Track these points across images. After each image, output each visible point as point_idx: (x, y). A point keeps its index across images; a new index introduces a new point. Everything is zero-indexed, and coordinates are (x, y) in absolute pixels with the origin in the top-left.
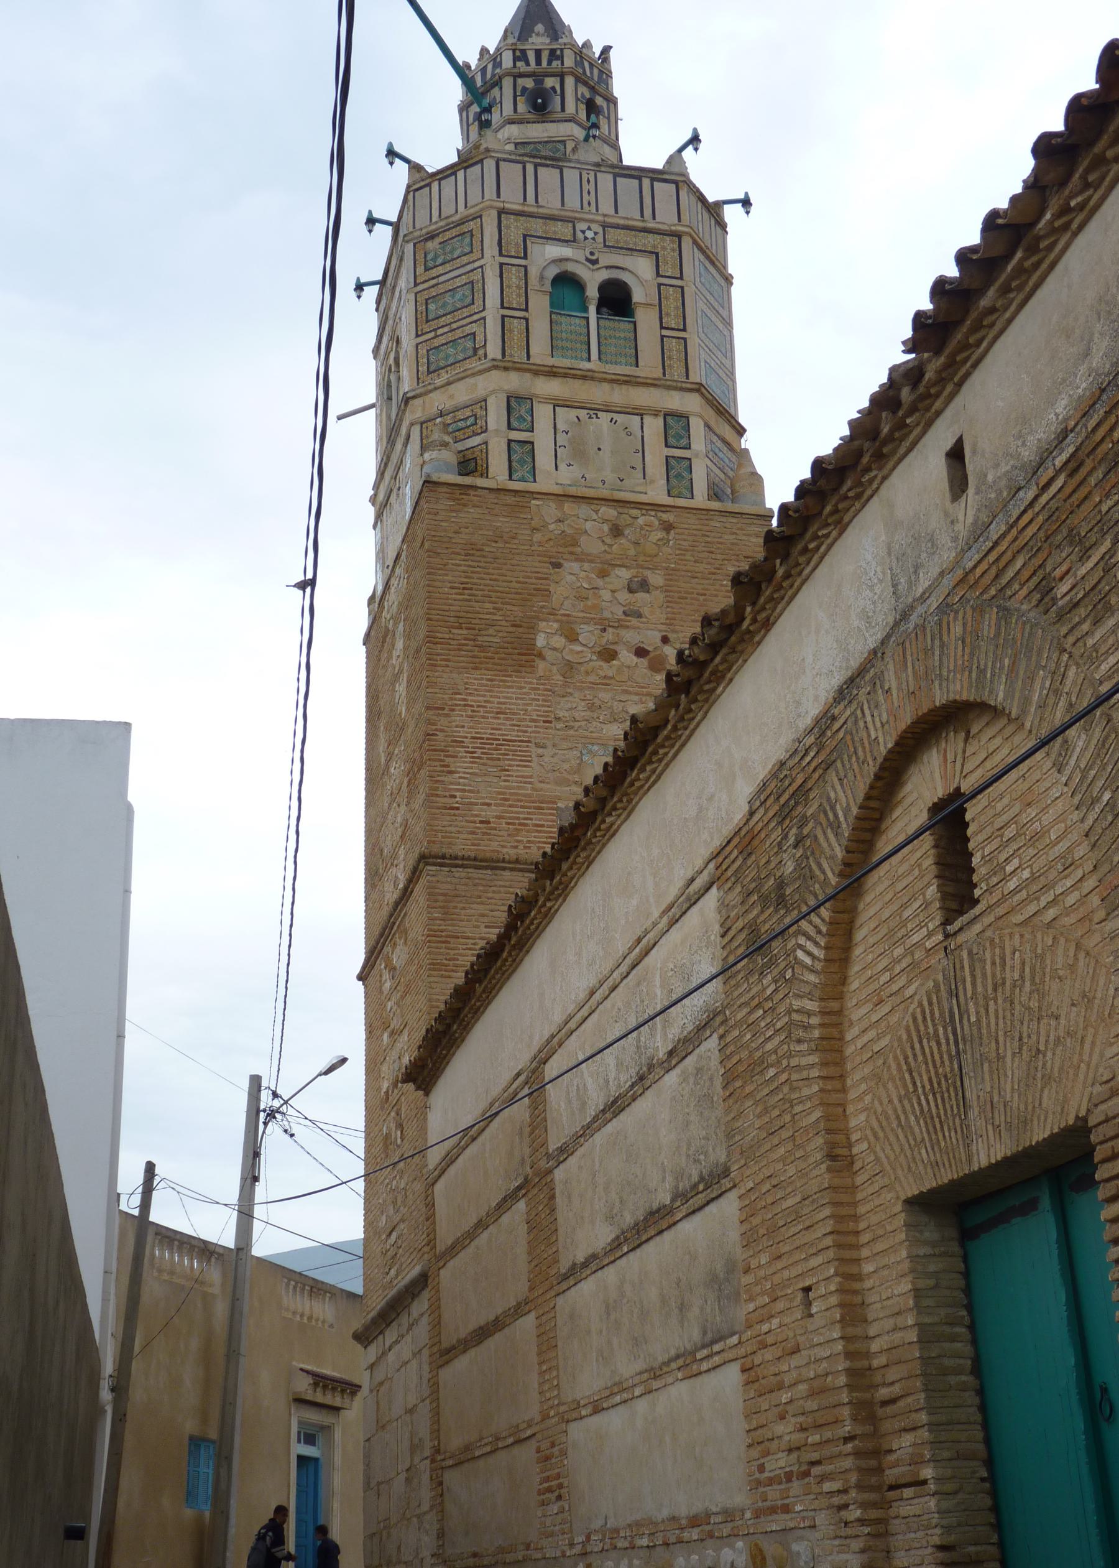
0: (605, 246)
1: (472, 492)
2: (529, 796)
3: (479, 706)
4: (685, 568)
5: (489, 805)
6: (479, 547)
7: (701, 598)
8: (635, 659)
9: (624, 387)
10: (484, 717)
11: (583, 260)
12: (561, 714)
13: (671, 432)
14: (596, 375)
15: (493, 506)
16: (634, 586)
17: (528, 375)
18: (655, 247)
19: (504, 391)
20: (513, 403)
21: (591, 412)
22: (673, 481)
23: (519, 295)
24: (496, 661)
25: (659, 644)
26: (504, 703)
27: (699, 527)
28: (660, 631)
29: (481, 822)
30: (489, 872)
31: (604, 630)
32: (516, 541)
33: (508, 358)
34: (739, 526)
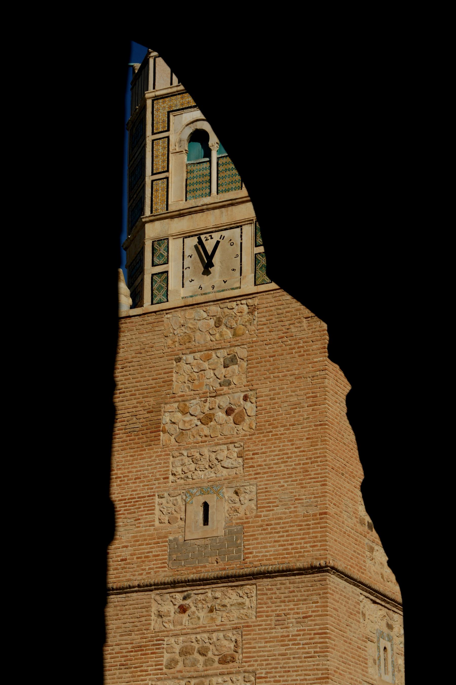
2: (152, 535)
3: (124, 477)
4: (262, 339)
5: (126, 547)
9: (230, 208)
10: (127, 484)
15: (140, 327)
16: (228, 362)
17: (167, 220)
20: (156, 246)
21: (207, 235)
23: (163, 161)
24: (137, 441)
25: (242, 402)
26: (140, 471)
29: (122, 560)
30: (124, 595)
32: (153, 349)
33: (155, 213)
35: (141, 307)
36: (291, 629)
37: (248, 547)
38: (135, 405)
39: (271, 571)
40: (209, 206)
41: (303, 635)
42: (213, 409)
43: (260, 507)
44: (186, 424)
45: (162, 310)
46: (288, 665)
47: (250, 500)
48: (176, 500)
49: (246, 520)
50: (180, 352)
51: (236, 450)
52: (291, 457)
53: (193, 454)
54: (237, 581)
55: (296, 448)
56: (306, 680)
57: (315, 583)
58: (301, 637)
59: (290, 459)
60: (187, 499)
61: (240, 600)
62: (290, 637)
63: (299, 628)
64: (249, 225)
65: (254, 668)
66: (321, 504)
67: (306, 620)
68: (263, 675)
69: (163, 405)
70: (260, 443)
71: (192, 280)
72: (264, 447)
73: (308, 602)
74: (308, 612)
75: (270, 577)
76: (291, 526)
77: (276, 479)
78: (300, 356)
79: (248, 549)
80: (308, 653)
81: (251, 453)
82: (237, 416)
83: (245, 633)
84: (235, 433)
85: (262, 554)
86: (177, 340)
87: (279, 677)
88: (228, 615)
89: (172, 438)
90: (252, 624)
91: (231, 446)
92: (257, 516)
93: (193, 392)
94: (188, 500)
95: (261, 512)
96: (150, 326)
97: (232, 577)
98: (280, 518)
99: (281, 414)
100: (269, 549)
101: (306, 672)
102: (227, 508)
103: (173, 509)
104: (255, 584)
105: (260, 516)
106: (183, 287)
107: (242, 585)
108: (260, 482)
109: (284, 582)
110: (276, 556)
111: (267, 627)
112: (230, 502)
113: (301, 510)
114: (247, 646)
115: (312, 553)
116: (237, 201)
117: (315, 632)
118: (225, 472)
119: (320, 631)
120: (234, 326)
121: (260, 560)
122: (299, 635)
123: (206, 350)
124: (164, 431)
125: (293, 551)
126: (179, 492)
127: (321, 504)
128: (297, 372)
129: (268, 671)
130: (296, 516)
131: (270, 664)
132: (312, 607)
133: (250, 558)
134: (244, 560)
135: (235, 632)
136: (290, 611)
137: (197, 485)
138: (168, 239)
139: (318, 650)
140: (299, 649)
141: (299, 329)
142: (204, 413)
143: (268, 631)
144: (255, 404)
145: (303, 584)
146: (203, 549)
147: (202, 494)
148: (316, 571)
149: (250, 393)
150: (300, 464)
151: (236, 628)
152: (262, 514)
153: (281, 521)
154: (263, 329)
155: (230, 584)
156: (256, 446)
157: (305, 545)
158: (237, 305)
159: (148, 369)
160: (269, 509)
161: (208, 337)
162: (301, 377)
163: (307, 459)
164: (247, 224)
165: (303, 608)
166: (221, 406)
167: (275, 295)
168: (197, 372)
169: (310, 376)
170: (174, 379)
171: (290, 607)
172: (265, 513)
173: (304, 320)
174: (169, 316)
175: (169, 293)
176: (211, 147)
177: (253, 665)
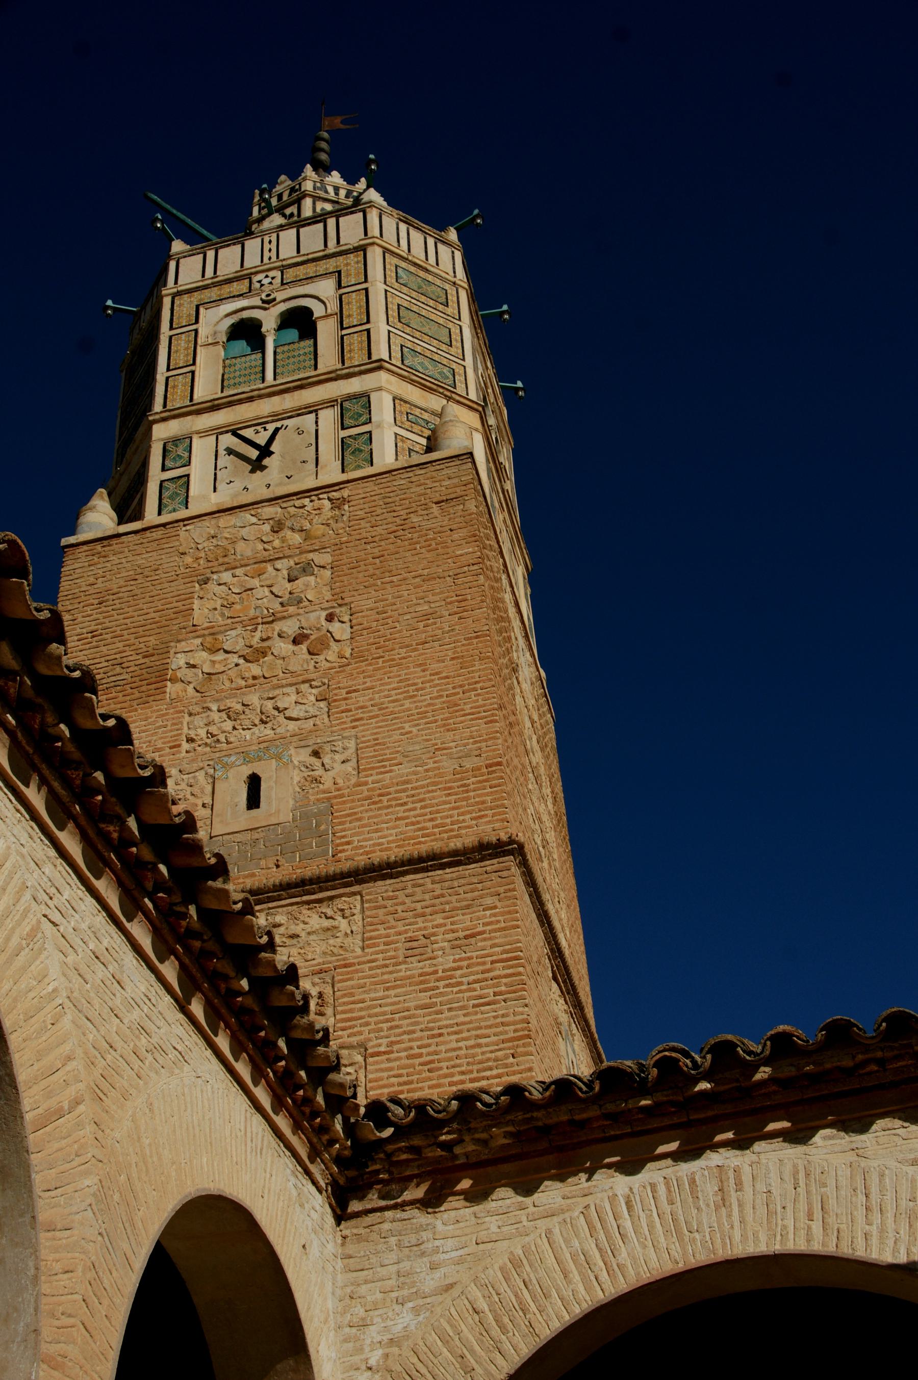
0: (282, 284)
1: (114, 541)
6: (115, 590)
7: (377, 561)
8: (291, 647)
11: (259, 303)
12: (192, 734)
13: (347, 415)
15: (136, 547)
17: (189, 418)
18: (337, 267)
19: (162, 439)
20: (170, 447)
21: (258, 428)
22: (349, 458)
24: (121, 699)
25: (324, 622)
32: (157, 572)
34: (428, 475)
35: (139, 520)
36: (440, 959)
37: (343, 833)
38: (122, 649)
39: (396, 862)
40: (263, 392)
41: (468, 967)
42: (268, 638)
43: (365, 770)
44: (217, 666)
45: (177, 521)
46: (437, 1024)
47: (343, 762)
48: (194, 777)
49: (337, 793)
50: (208, 571)
51: (314, 691)
52: (422, 689)
53: (229, 705)
54: (321, 890)
56: (479, 1046)
57: (486, 876)
58: (465, 971)
59: (420, 692)
60: (217, 773)
61: (327, 923)
62: (440, 974)
63: (457, 957)
65: (362, 1037)
66: (487, 752)
67: (473, 940)
68: (382, 1049)
69: (172, 644)
70: (361, 676)
72: (368, 680)
73: (475, 909)
74: (475, 926)
75: (391, 876)
76: (429, 792)
77: (394, 724)
78: (429, 551)
79: (343, 837)
80: (481, 997)
81: (344, 691)
82: (314, 643)
83: (340, 977)
84: (311, 667)
85: (371, 842)
86: (202, 554)
87: (419, 1047)
88: (302, 951)
89: (190, 689)
90: (356, 961)
91: (304, 687)
92: (359, 785)
93: (230, 621)
94: (218, 774)
95: (367, 776)
96: (155, 544)
97: (311, 881)
98: (407, 782)
99: (400, 631)
100: (386, 832)
101: (479, 1032)
102: (296, 779)
103: (189, 792)
104: (359, 893)
105: (366, 783)
106: (215, 491)
107: (331, 898)
108: (363, 731)
109: (421, 881)
110: (402, 843)
111: (388, 962)
112: (303, 769)
113: (449, 765)
114: (346, 1000)
115: (476, 828)
117: (494, 958)
118: (292, 725)
119: (505, 956)
120: (307, 526)
121: (367, 853)
122: (460, 968)
123: (255, 563)
124: (173, 680)
125: (436, 830)
126: (201, 765)
127: (487, 752)
128: (426, 572)
129: (393, 1039)
130: (441, 775)
131: (397, 1027)
132: (485, 916)
133: (347, 850)
134: (333, 856)
135: (317, 980)
136: (435, 930)
137: (237, 751)
138: (191, 438)
139: (503, 988)
140: (460, 991)
142: (251, 647)
143: (391, 969)
144: (348, 624)
145: (462, 881)
146: (248, 848)
147: (247, 761)
148: (490, 855)
149: (337, 610)
150: (441, 696)
151: (320, 972)
152: (370, 779)
153: (410, 786)
154: (360, 524)
155: (305, 898)
156: (354, 680)
157: (461, 818)
158: (311, 501)
159: (148, 599)
160: (382, 770)
161: (260, 546)
162: (435, 578)
163: (454, 688)
164: (327, 407)
165: (464, 921)
166: (284, 632)
167: (379, 481)
168: (239, 594)
169: (451, 574)
170: (195, 607)
171: (435, 923)
172: (375, 778)
173: (434, 505)
174: (188, 528)
177: (360, 1033)
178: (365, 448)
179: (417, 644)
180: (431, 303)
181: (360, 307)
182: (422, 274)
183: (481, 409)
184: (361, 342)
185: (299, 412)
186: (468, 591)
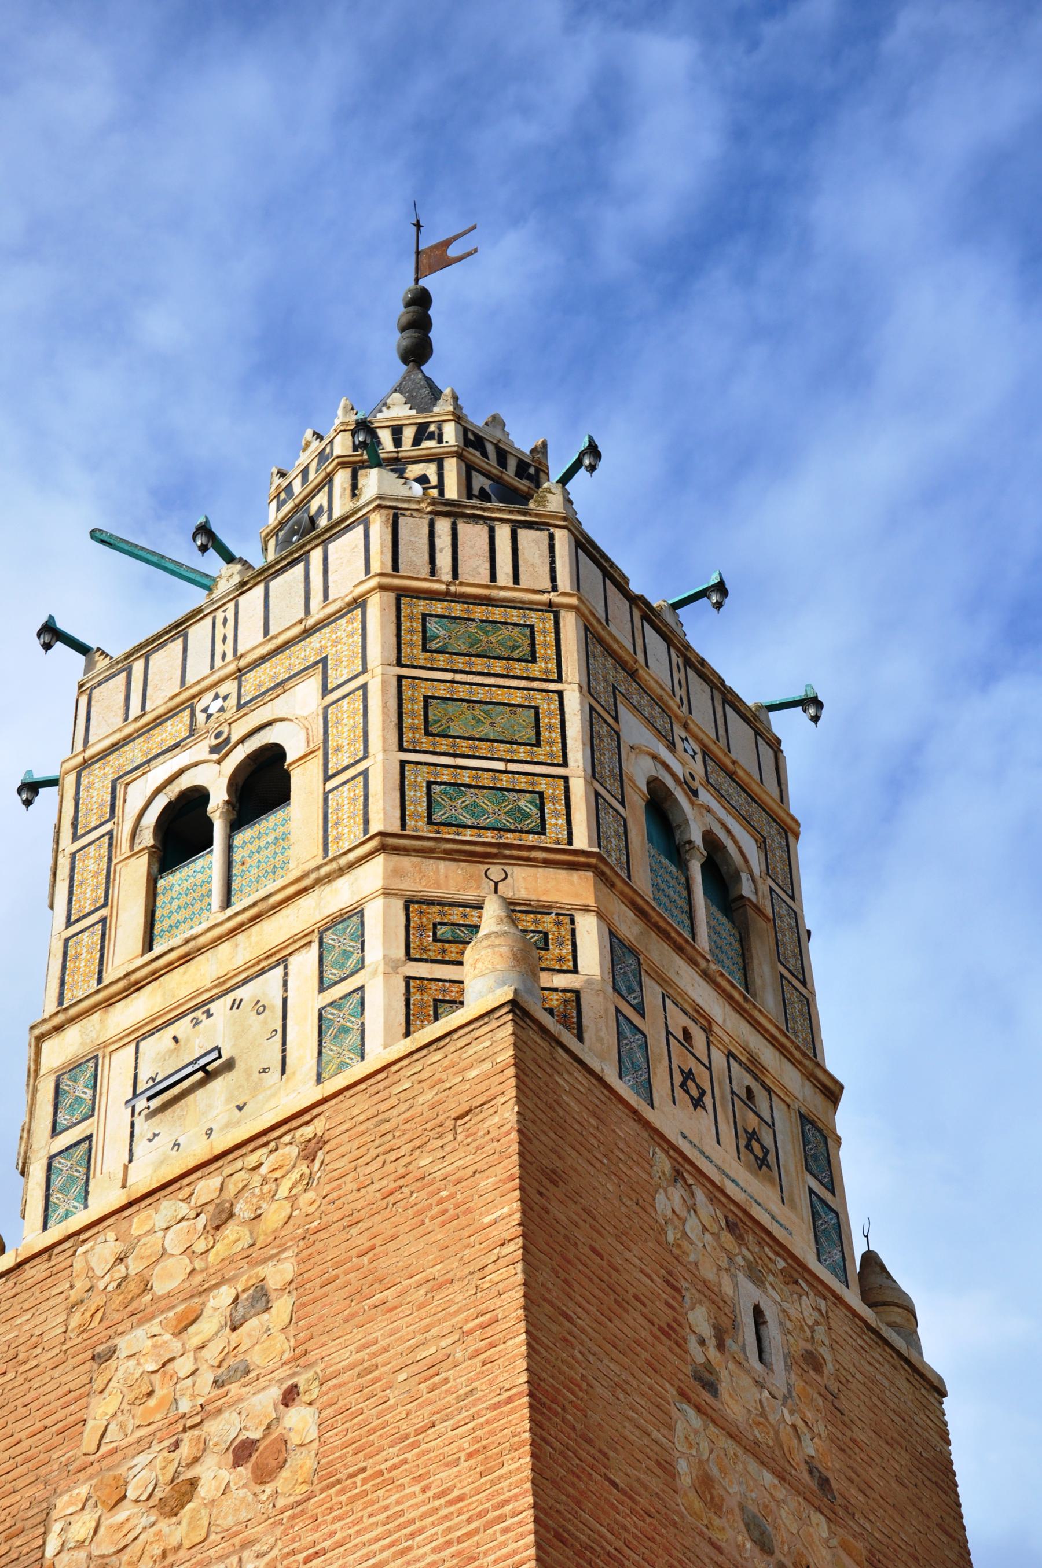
14: (202, 940)
21: (198, 1014)
27: (373, 1111)
28: (281, 1381)
31: (177, 1445)
34: (446, 1062)
52: (421, 1531)
55: (437, 1497)
59: (418, 1539)
64: (304, 951)
71: (155, 1135)
116: (272, 900)
138: (96, 1057)
141: (440, 1153)
149: (301, 1381)
154: (339, 1187)
163: (469, 1521)
175: (90, 1189)
176: (211, 816)
178: (354, 1024)
179: (418, 1432)
180: (498, 667)
181: (355, 725)
182: (479, 612)
183: (593, 861)
184: (353, 801)
185: (258, 970)
186: (498, 1302)
